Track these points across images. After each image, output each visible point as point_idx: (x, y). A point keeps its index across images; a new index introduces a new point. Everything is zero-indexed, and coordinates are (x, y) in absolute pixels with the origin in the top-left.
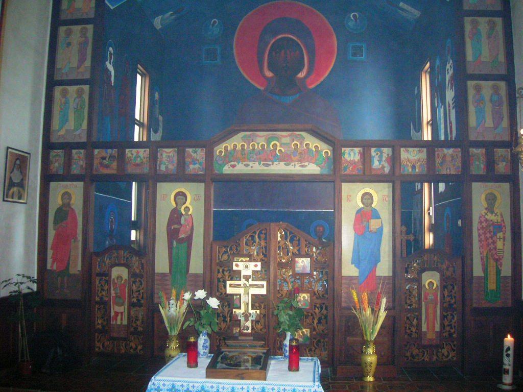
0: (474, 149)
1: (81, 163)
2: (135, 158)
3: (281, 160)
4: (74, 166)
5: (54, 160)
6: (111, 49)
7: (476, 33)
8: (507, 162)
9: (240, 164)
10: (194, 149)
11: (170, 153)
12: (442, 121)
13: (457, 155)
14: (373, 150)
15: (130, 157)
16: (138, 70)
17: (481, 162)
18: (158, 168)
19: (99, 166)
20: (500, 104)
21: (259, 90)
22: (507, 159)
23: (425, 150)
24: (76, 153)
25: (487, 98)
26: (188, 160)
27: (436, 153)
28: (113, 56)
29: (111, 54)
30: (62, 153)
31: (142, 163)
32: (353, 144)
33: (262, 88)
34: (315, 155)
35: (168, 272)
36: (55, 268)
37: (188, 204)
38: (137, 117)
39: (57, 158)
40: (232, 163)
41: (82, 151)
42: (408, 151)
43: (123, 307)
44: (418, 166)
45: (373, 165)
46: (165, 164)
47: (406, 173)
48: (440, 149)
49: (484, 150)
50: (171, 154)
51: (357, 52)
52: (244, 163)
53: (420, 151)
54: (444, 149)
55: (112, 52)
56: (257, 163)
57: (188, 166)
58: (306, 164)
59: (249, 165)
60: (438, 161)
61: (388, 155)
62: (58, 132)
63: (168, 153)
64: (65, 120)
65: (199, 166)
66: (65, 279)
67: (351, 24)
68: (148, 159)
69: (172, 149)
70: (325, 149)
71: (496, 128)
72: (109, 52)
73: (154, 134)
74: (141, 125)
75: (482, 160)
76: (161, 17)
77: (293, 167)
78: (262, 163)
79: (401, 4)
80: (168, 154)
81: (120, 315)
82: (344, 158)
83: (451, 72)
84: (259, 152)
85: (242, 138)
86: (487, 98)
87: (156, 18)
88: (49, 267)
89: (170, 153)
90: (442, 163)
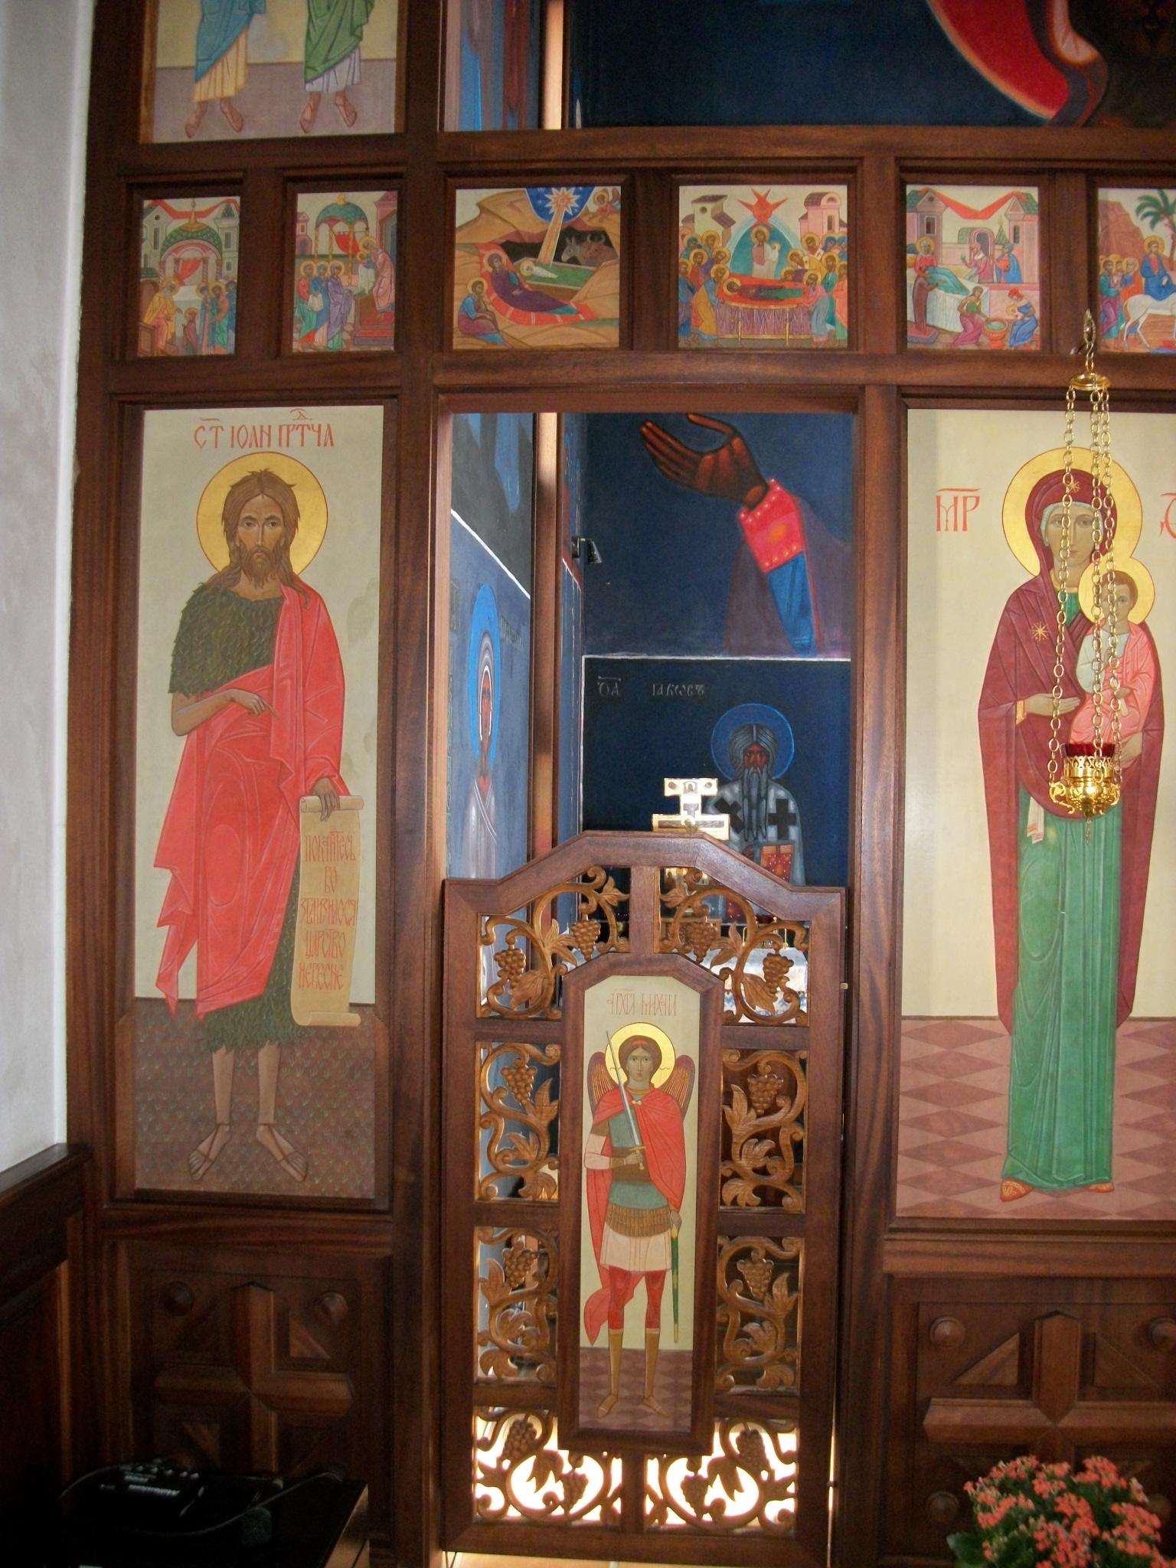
1: (363, 279)
2: (744, 243)
4: (316, 302)
5: (170, 269)
10: (1154, 193)
15: (712, 238)
18: (910, 316)
19: (490, 299)
24: (328, 218)
26: (1116, 265)
30: (227, 214)
31: (798, 275)
33: (1046, 113)
35: (994, 1012)
36: (187, 986)
37: (1121, 557)
39: (190, 253)
41: (368, 201)
43: (662, 1240)
46: (962, 289)
50: (998, 224)
57: (1114, 302)
62: (198, 79)
63: (974, 215)
66: (266, 1058)
69: (1001, 192)
80: (978, 224)
81: (641, 1290)
88: (145, 984)
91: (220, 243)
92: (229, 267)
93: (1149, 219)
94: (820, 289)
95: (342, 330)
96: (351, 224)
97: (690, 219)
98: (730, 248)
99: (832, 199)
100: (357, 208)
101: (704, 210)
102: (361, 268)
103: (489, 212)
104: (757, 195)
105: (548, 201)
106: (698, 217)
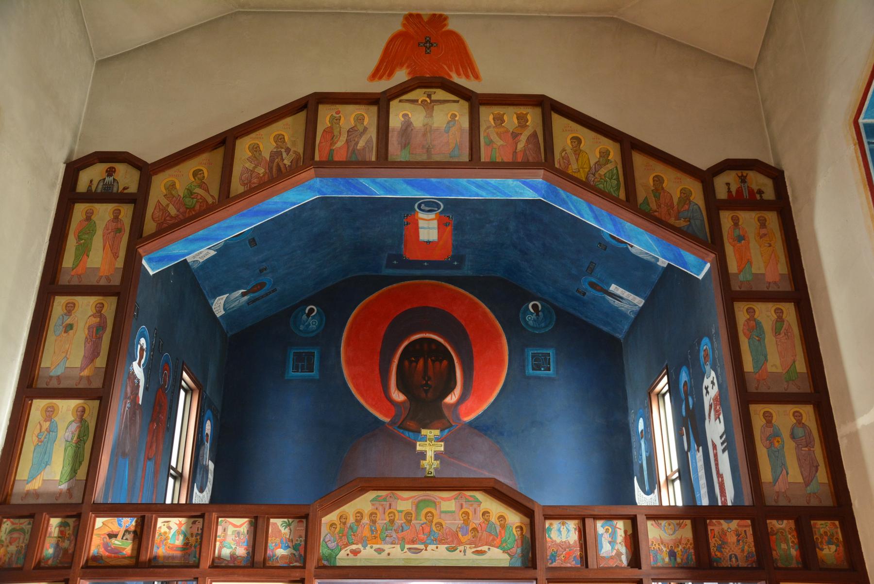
0: (774, 522)
3: (440, 541)
6: (143, 341)
7: (755, 327)
8: (837, 546)
9: (368, 548)
11: (241, 526)
12: (702, 473)
13: (745, 531)
14: (599, 524)
15: (165, 533)
16: (183, 383)
17: (791, 544)
20: (809, 444)
21: (383, 423)
22: (837, 539)
23: (688, 522)
25: (786, 434)
27: (710, 528)
28: (145, 353)
29: (142, 349)
30: (29, 524)
32: (561, 514)
33: (387, 420)
34: (500, 532)
38: (173, 463)
40: (354, 547)
42: (659, 525)
44: (680, 553)
45: (601, 550)
46: (232, 547)
47: (660, 564)
48: (714, 521)
49: (792, 523)
51: (540, 363)
52: (376, 546)
53: (679, 525)
54: (722, 521)
55: (145, 347)
56: (398, 547)
58: (485, 548)
59: (383, 550)
60: (713, 542)
61: (625, 532)
64: (44, 461)
65: (295, 552)
67: (530, 318)
68: (198, 537)
70: (514, 519)
71: (807, 484)
72: (139, 346)
73: (198, 493)
74: (179, 477)
75: (793, 542)
76: (226, 296)
77: (462, 553)
78: (407, 546)
79: (613, 288)
82: (551, 538)
83: (714, 391)
84: (402, 526)
85: (370, 501)
86: (786, 434)
87: (218, 298)
89: (241, 526)
90: (720, 548)
91: (25, 532)
92: (26, 540)
93: (284, 527)
94: (193, 548)
95: (57, 559)
96: (65, 527)
97: (160, 527)
98: (170, 536)
99: (199, 522)
100: (67, 523)
101: (164, 525)
102: (66, 541)
103: (106, 525)
104: (179, 521)
105: (122, 522)
106: (163, 527)
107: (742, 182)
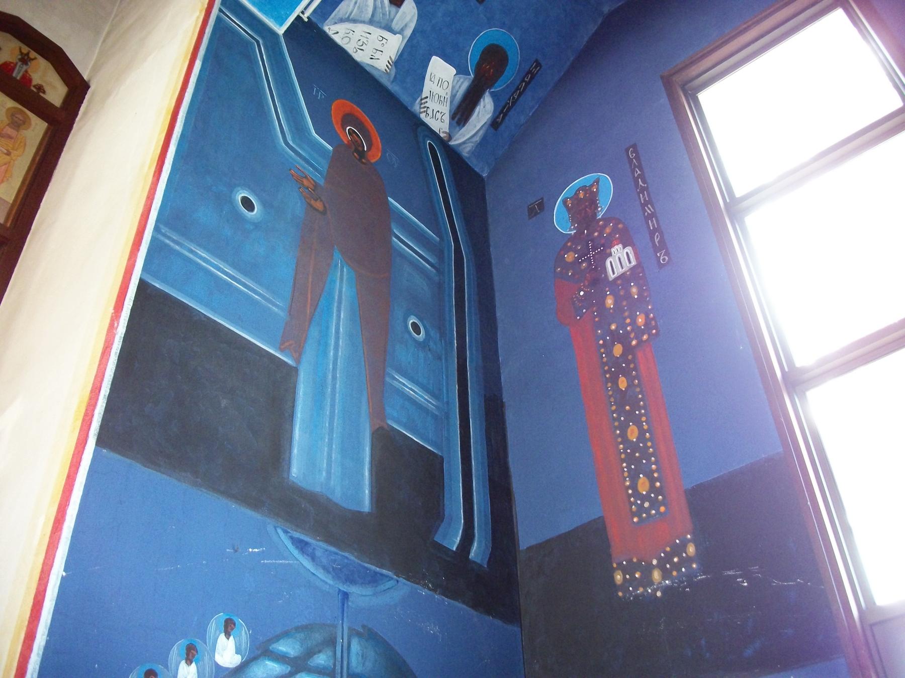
107: (21, 60)
